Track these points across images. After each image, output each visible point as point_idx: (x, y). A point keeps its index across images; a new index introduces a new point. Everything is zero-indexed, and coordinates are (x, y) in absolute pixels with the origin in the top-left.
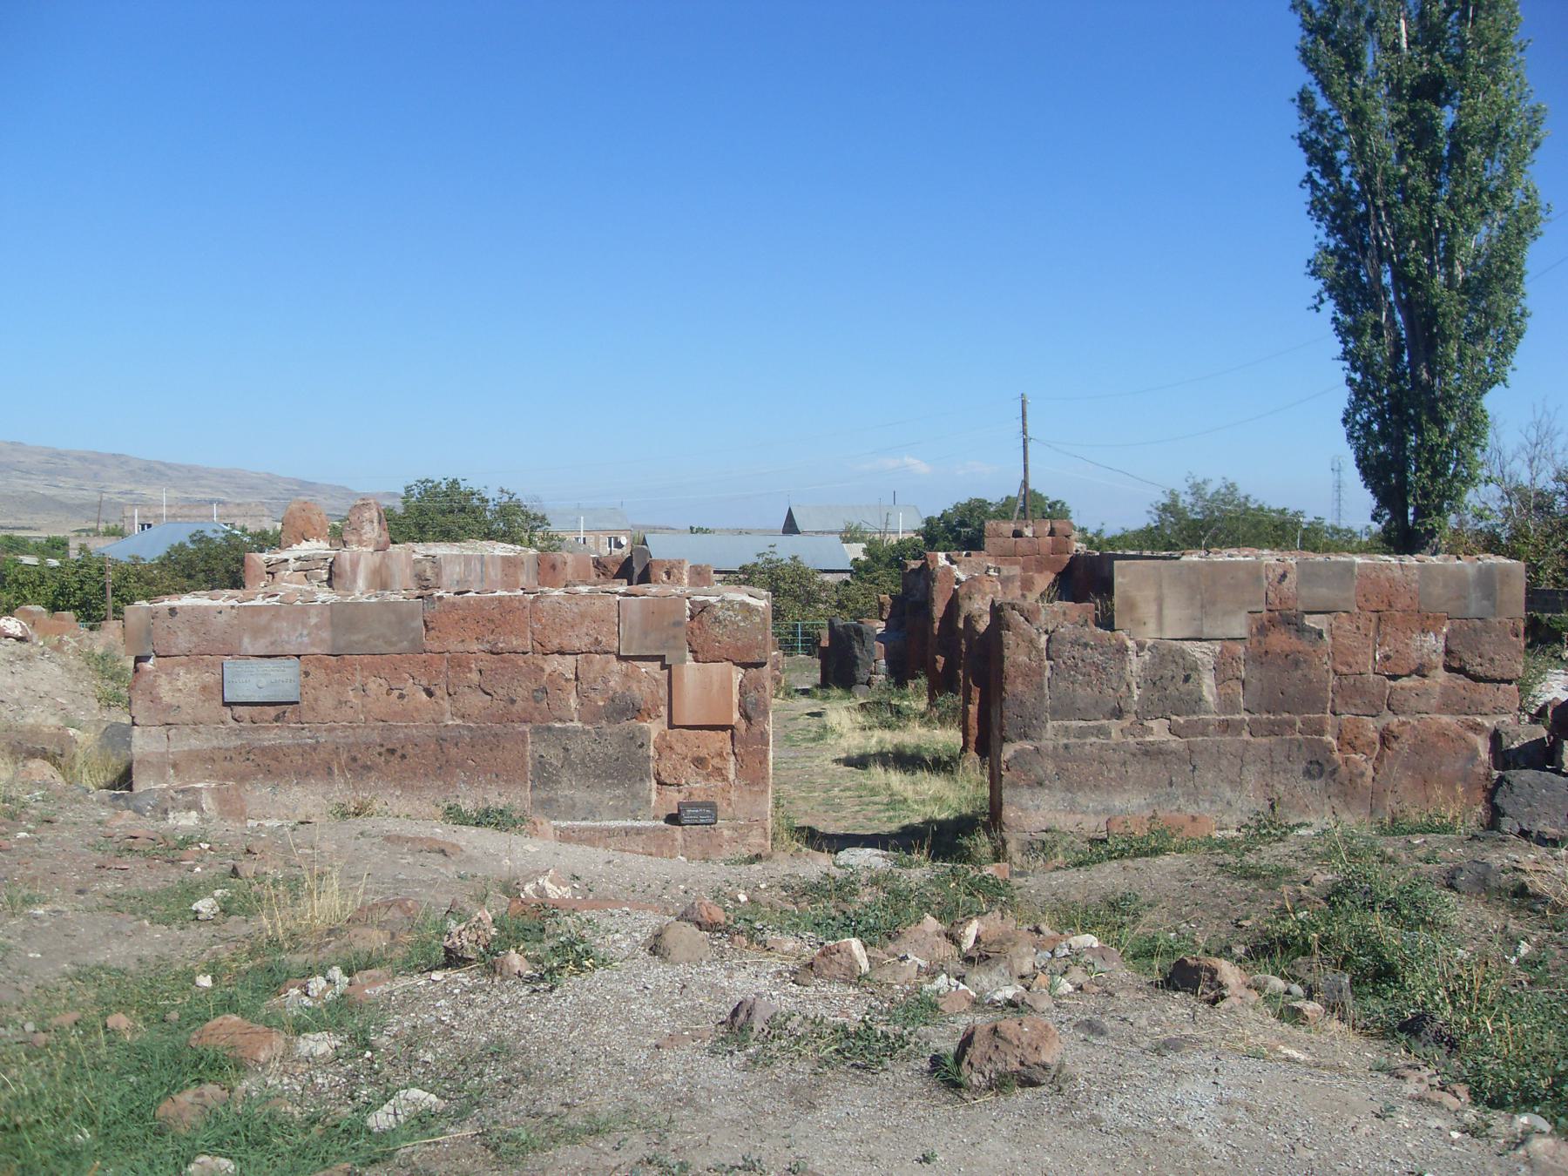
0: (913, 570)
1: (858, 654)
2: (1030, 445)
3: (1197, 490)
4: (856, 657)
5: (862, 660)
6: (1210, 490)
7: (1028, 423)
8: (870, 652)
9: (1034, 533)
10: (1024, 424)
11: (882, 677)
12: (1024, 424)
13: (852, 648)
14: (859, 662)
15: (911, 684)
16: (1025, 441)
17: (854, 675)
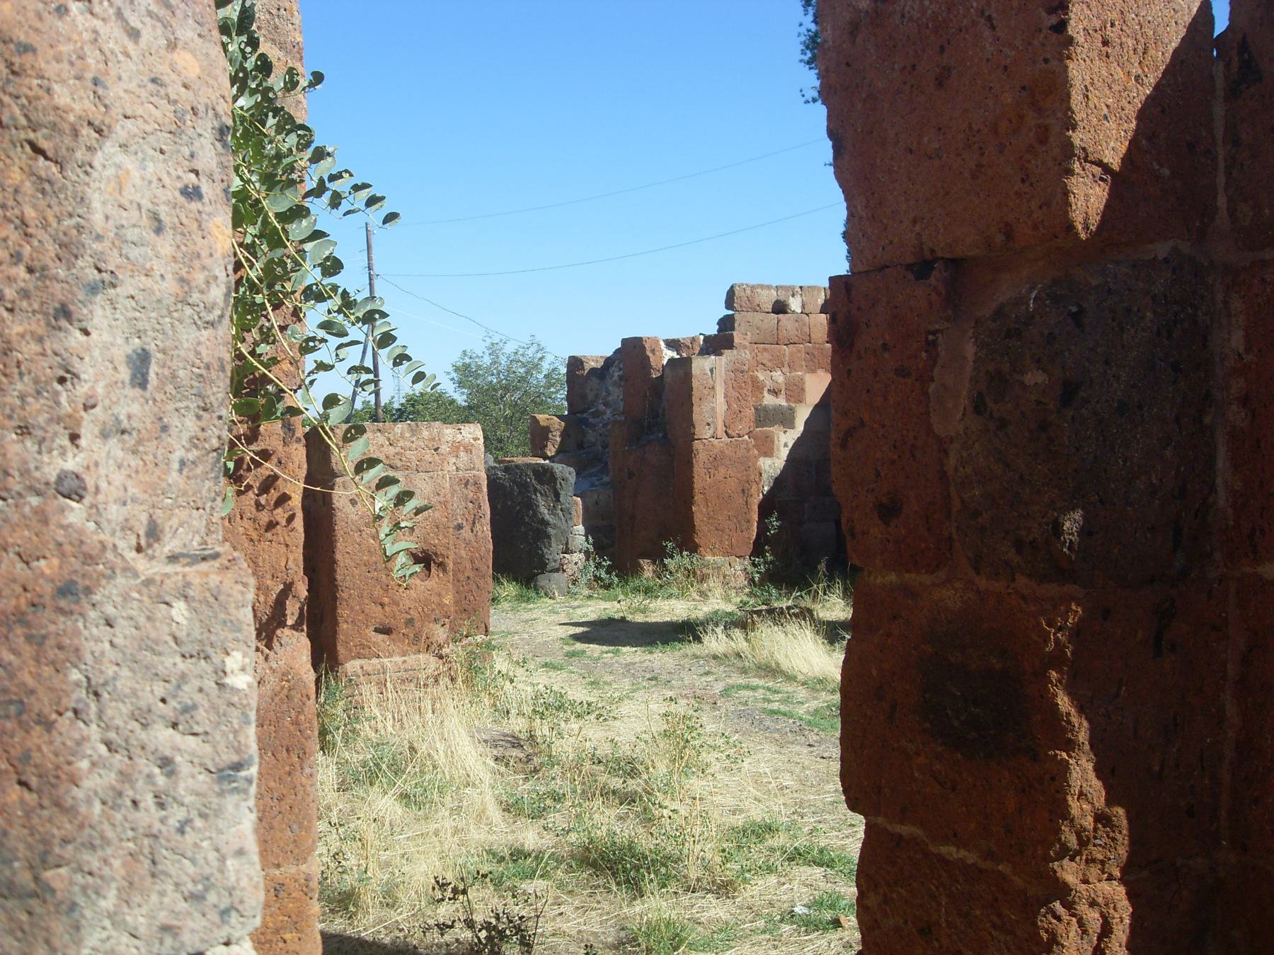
0: (593, 370)
1: (547, 517)
2: (376, 282)
3: (494, 350)
4: (545, 523)
5: (555, 527)
6: (509, 348)
7: (374, 256)
8: (567, 512)
9: (803, 306)
10: (369, 259)
11: (578, 557)
12: (369, 259)
13: (531, 506)
14: (551, 531)
15: (648, 569)
16: (370, 279)
17: (543, 556)
